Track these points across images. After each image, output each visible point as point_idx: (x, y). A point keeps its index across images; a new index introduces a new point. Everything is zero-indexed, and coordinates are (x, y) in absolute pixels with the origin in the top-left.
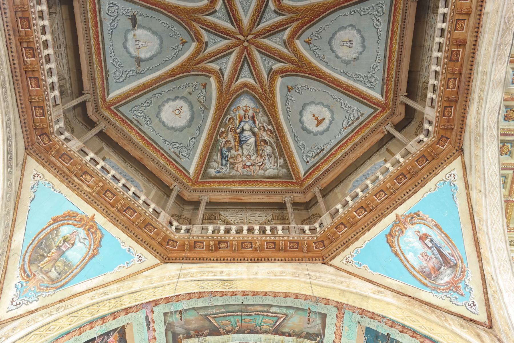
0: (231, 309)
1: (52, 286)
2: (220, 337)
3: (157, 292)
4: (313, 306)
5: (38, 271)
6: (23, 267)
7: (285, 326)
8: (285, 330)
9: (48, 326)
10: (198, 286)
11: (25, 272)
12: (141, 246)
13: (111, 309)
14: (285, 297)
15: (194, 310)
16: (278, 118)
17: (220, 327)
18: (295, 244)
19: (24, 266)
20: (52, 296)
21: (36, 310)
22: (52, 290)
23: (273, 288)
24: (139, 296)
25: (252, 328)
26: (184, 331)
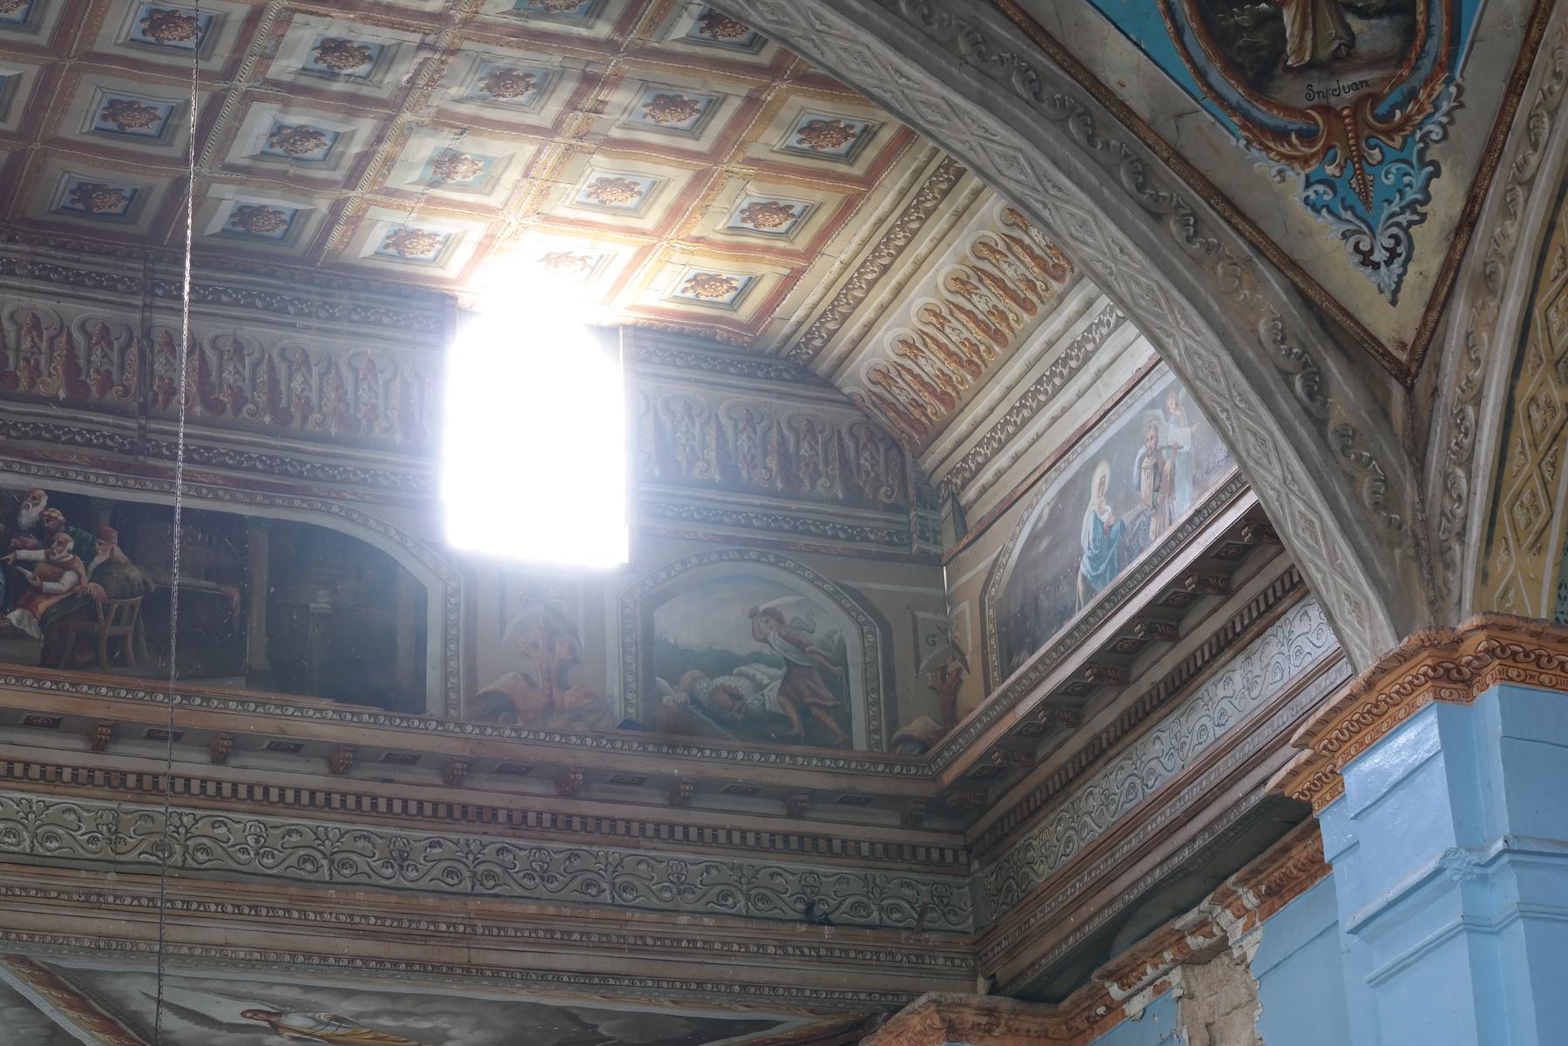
1: (1423, 73)
5: (1316, 87)
6: (1249, 123)
11: (1281, 135)
19: (1253, 121)
20: (1461, 105)
21: (1474, 200)
22: (1439, 88)
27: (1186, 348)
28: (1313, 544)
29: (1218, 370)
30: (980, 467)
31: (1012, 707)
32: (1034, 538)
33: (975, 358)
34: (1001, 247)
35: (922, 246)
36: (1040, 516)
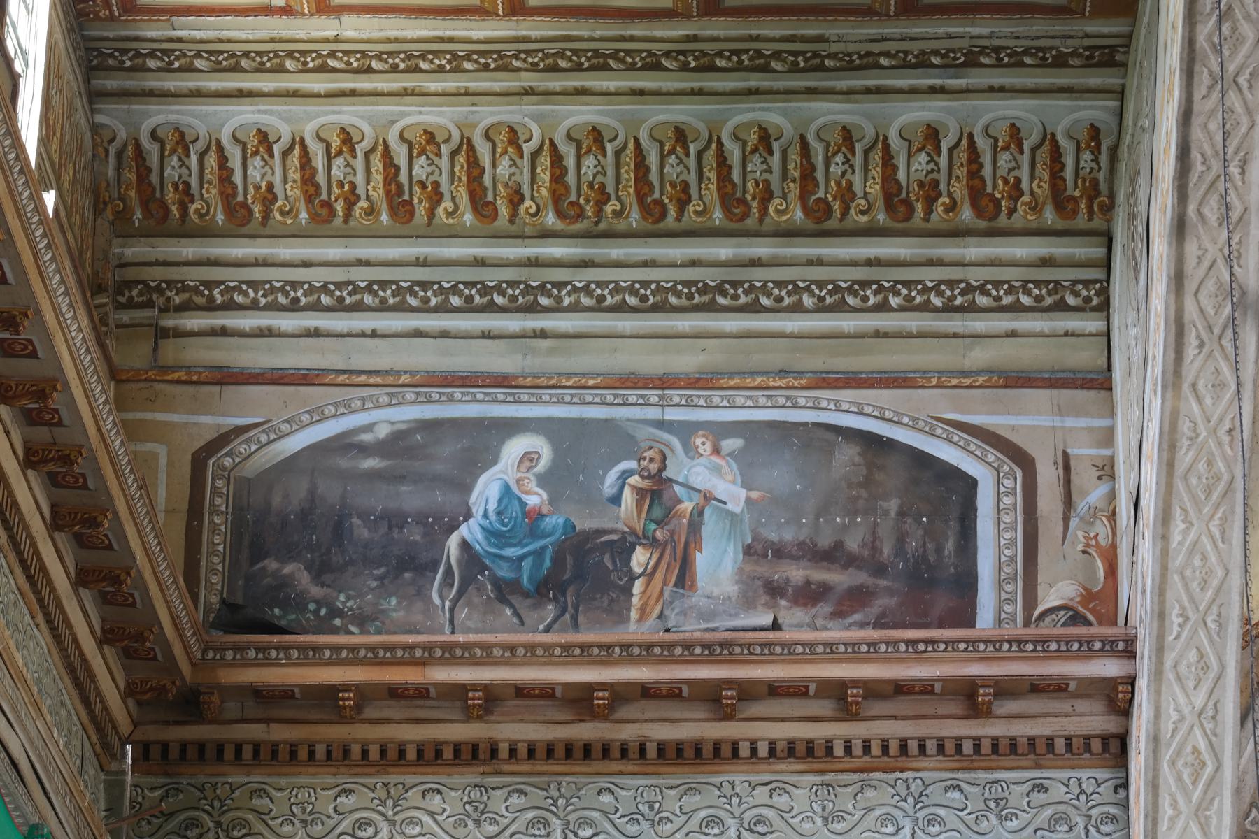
27: (1195, 543)
28: (1187, 779)
29: (1215, 583)
30: (230, 306)
31: (423, 663)
32: (343, 444)
33: (339, 207)
34: (528, 148)
35: (434, 85)
36: (369, 428)
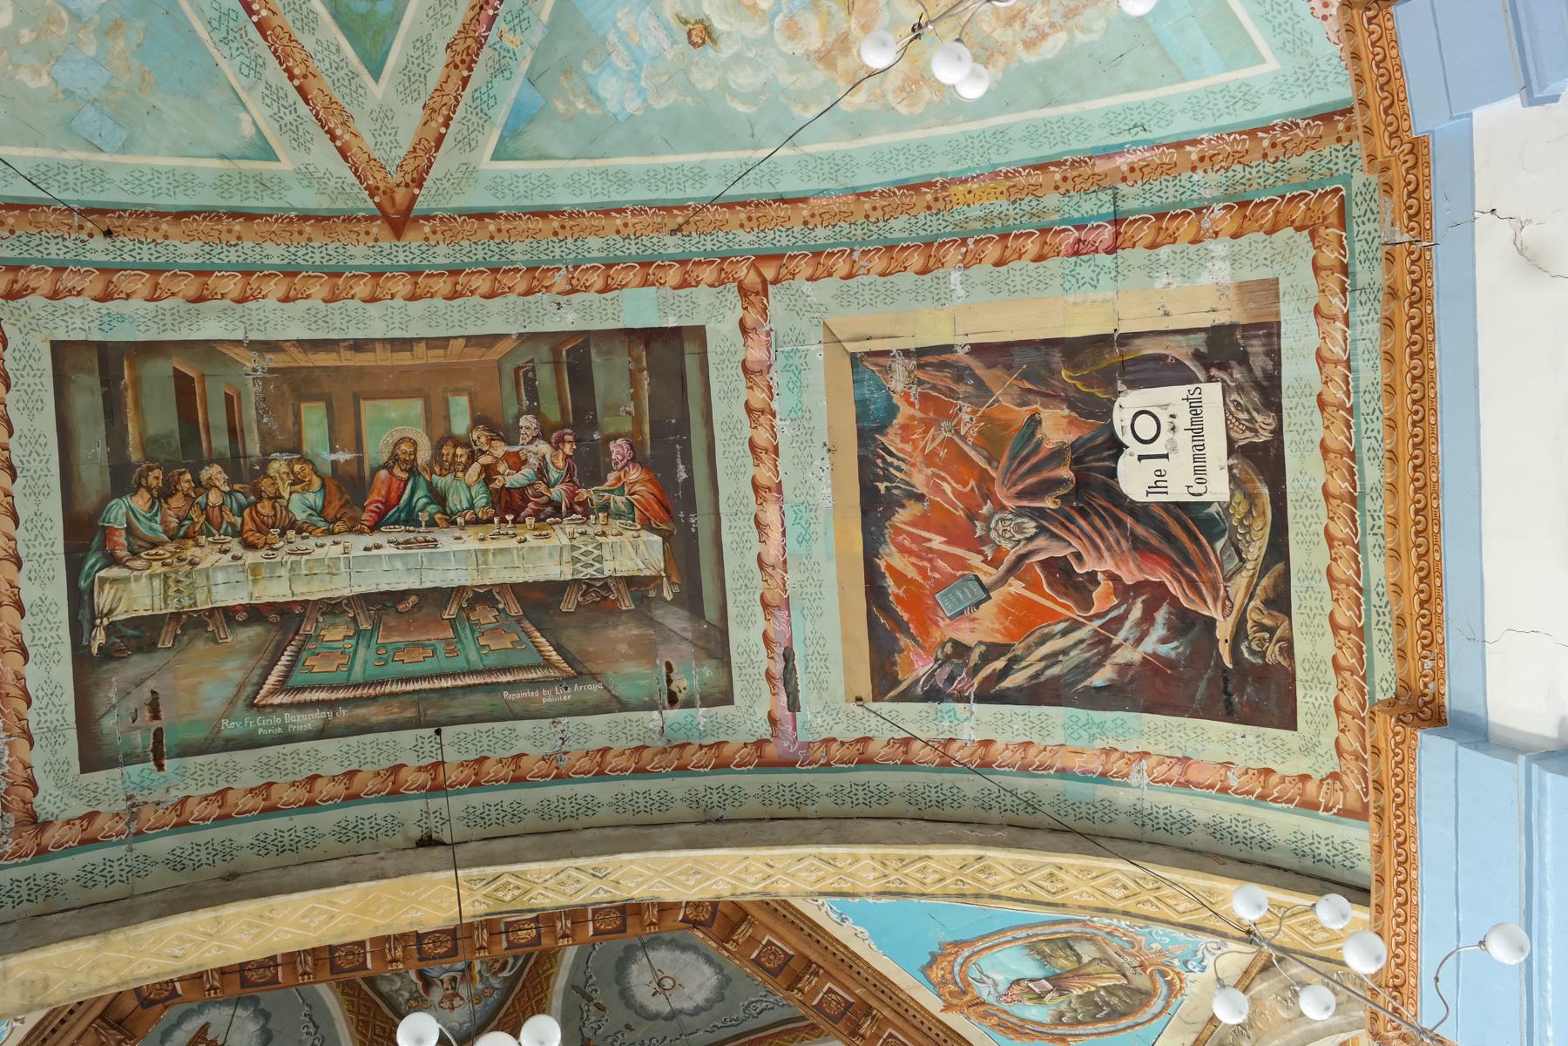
0: (480, 701)
2: (518, 577)
3: (759, 876)
4: (144, 784)
7: (256, 651)
8: (249, 634)
9: (1130, 905)
10: (613, 877)
11: (1170, 984)
12: (803, 915)
13: (920, 858)
14: (270, 784)
15: (623, 699)
16: (343, 993)
17: (519, 622)
18: (254, 976)
23: (330, 903)
24: (821, 873)
25: (392, 620)
26: (658, 613)
